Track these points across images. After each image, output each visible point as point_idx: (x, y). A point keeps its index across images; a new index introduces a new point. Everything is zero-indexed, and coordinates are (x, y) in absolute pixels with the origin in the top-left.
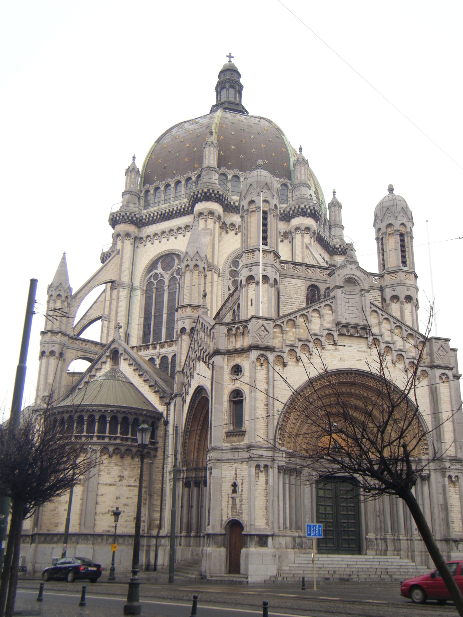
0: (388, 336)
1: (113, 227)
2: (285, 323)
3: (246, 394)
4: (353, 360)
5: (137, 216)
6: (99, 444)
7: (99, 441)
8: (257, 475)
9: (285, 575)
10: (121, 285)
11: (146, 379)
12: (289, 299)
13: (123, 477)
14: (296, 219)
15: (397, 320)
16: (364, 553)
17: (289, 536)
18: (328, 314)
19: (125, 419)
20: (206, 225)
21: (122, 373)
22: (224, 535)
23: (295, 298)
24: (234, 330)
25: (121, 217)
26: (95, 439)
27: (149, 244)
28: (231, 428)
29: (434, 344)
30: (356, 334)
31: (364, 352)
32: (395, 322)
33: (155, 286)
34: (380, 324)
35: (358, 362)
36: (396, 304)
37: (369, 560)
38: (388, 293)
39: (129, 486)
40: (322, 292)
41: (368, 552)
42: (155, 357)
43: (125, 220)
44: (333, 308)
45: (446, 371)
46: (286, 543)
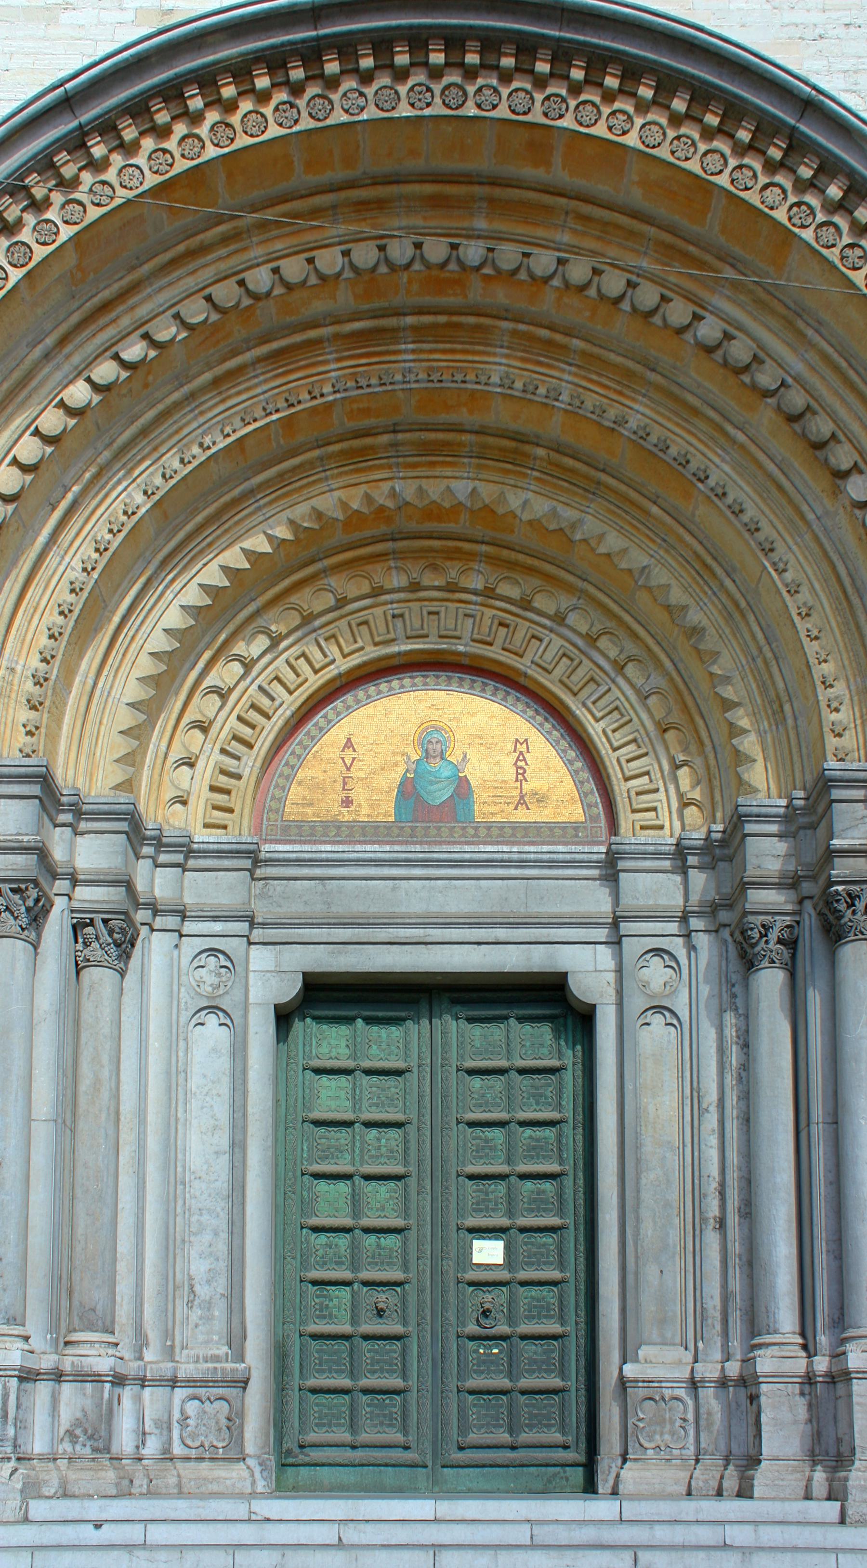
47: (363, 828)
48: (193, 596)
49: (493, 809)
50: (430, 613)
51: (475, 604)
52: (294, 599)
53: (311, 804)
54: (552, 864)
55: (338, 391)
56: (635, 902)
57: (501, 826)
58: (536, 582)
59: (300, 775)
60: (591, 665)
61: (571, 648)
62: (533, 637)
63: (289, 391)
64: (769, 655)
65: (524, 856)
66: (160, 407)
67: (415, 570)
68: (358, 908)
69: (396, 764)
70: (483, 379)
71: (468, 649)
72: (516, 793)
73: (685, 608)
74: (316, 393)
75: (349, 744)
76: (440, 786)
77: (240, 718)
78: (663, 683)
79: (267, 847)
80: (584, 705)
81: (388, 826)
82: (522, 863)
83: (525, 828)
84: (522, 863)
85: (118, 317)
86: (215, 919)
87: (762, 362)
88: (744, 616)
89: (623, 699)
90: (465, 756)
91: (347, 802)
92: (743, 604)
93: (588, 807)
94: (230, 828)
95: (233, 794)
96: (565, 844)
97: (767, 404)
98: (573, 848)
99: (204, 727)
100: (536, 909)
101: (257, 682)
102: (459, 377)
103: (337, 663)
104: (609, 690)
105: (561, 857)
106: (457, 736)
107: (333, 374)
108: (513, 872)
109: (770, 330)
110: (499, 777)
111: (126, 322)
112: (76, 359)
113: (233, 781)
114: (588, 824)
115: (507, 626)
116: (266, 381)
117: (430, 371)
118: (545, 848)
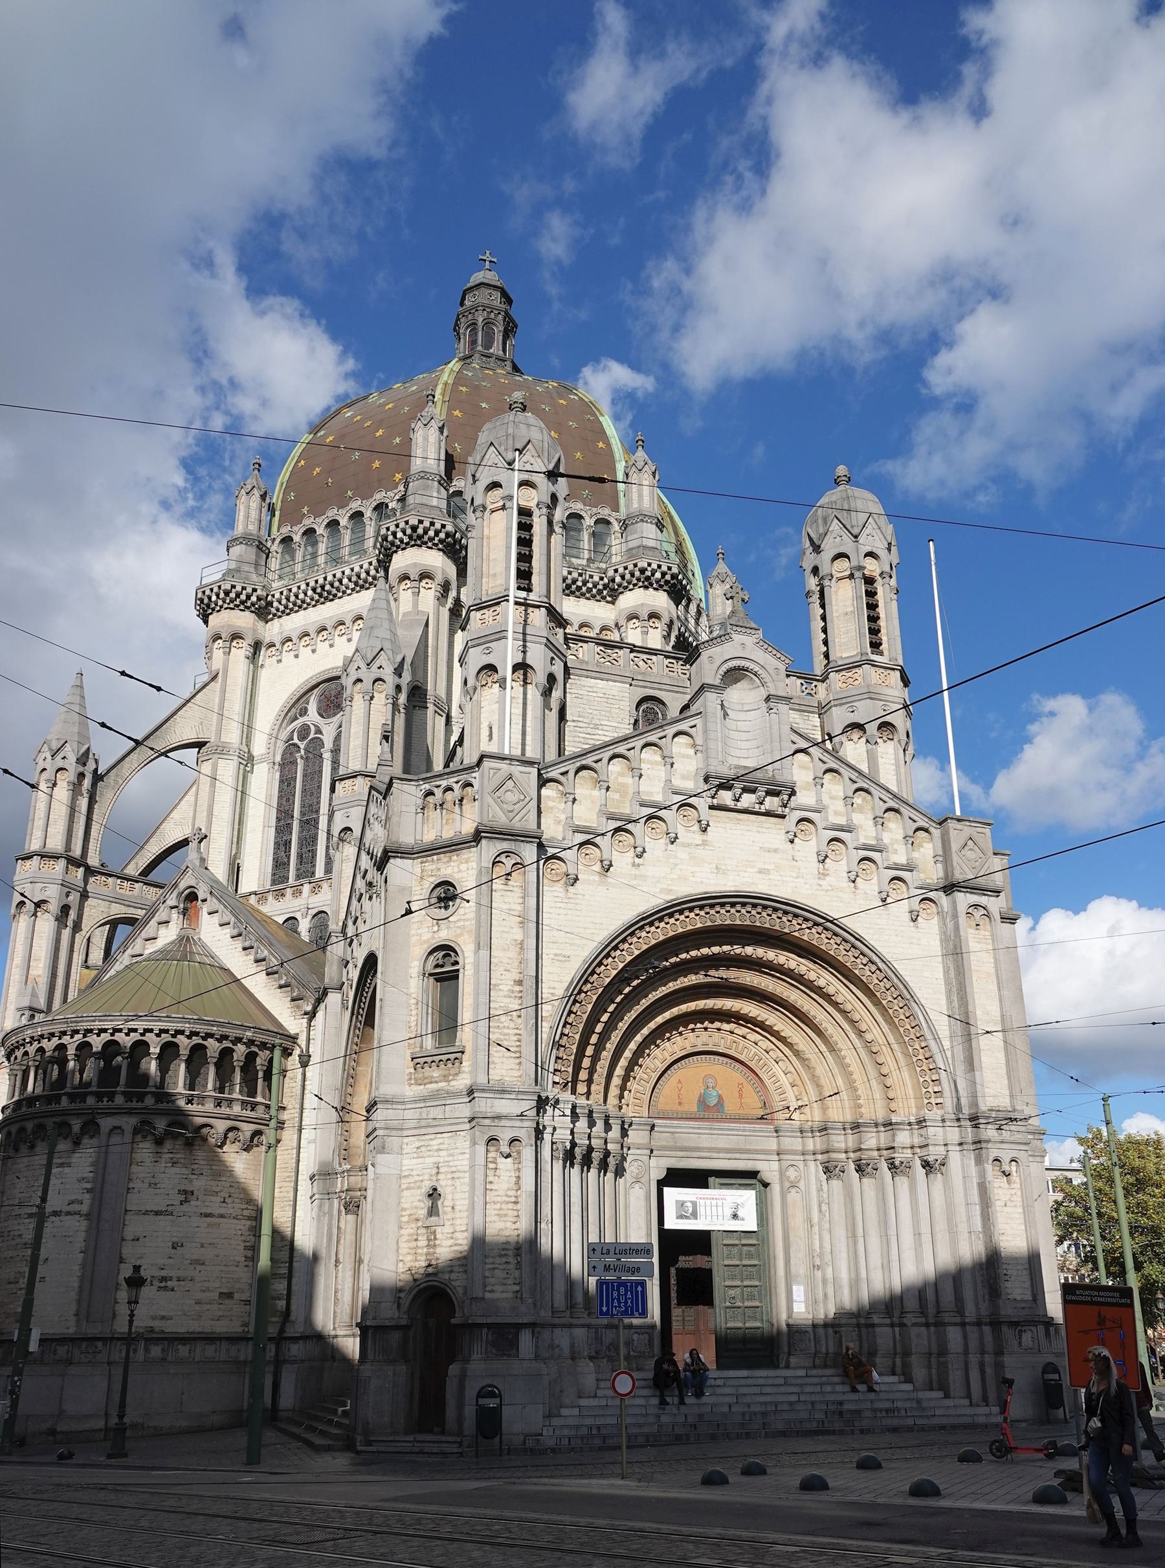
0: (836, 813)
1: (206, 622)
2: (571, 774)
3: (466, 955)
4: (749, 870)
5: (259, 592)
6: (130, 1112)
7: (129, 1105)
8: (491, 1166)
9: (566, 1432)
10: (222, 751)
11: (260, 956)
12: (589, 730)
13: (192, 1192)
14: (628, 594)
15: (860, 773)
16: (783, 1364)
17: (583, 1326)
18: (684, 756)
19: (198, 1052)
20: (416, 604)
21: (204, 946)
22: (406, 1328)
23: (605, 728)
24: (438, 792)
25: (222, 595)
26: (119, 1100)
27: (287, 657)
28: (429, 1043)
29: (953, 833)
30: (757, 806)
31: (776, 851)
32: (854, 778)
33: (302, 752)
34: (818, 782)
35: (762, 876)
36: (858, 746)
37: (793, 1381)
38: (839, 718)
39: (207, 1215)
40: (673, 711)
41: (793, 1360)
42: (298, 916)
43: (232, 601)
44: (699, 741)
45: (983, 900)
46: (572, 1346)
82: (744, 1131)
91: (680, 1104)
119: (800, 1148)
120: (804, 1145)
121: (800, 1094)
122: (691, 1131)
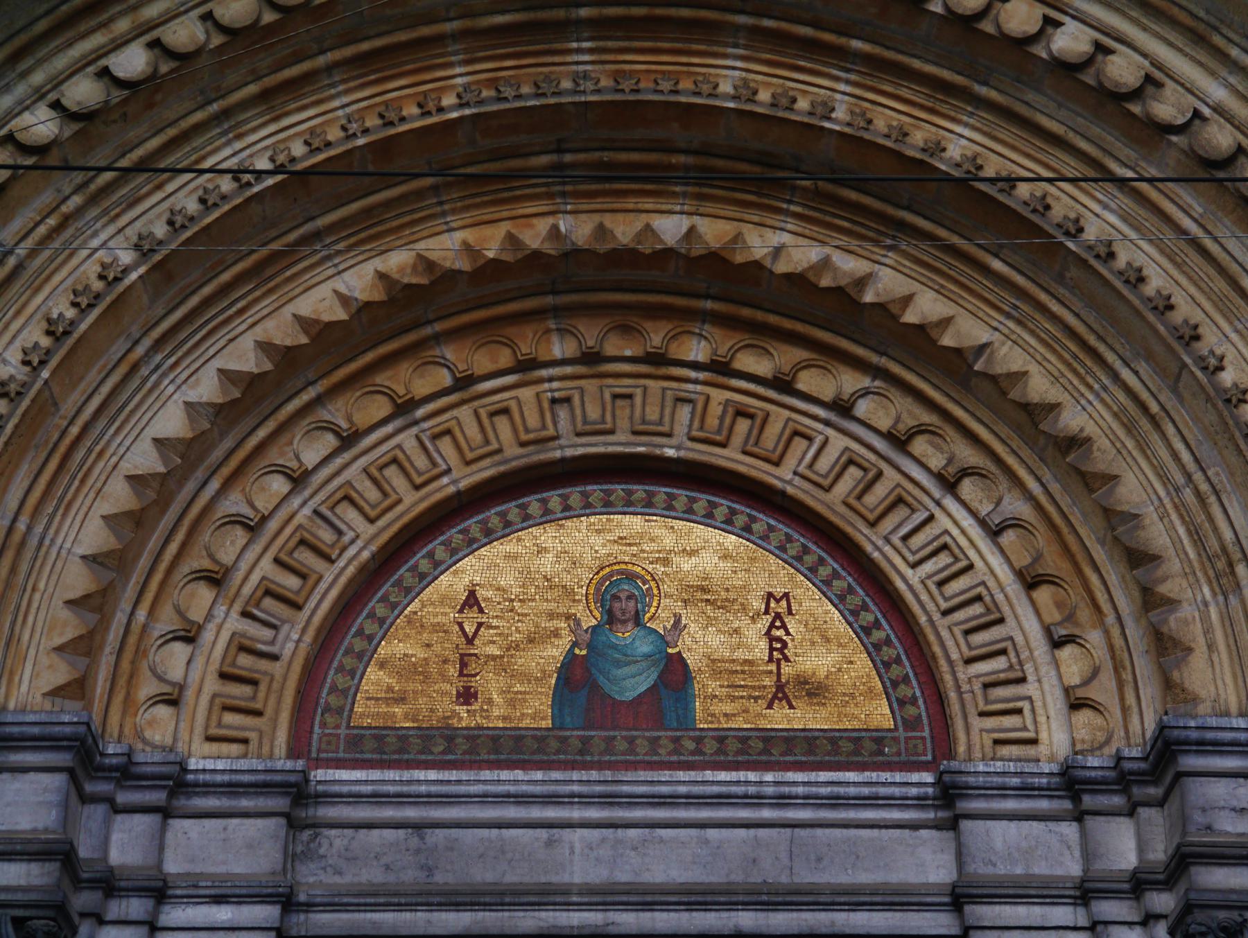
47: (495, 739)
48: (206, 388)
49: (728, 708)
50: (616, 397)
51: (696, 382)
52: (381, 379)
53: (401, 700)
54: (836, 802)
55: (467, 105)
56: (989, 870)
57: (744, 738)
58: (800, 354)
59: (383, 651)
60: (898, 477)
61: (863, 451)
62: (796, 433)
63: (386, 103)
64: (1204, 487)
65: (786, 790)
66: (172, 132)
67: (591, 333)
68: (484, 875)
69: (556, 634)
70: (706, 88)
71: (682, 454)
72: (767, 681)
73: (1054, 407)
74: (431, 106)
75: (472, 601)
76: (632, 669)
77: (277, 561)
78: (1023, 510)
79: (320, 774)
80: (887, 540)
81: (540, 737)
82: (783, 800)
83: (786, 739)
84: (783, 800)
85: (111, 20)
86: (219, 900)
87: (1159, 85)
88: (1157, 425)
89: (955, 532)
90: (678, 619)
92: (1154, 408)
93: (899, 704)
94: (253, 746)
95: (263, 687)
96: (861, 767)
97: (1170, 143)
98: (873, 776)
99: (216, 579)
100: (806, 876)
101: (312, 504)
102: (666, 85)
103: (455, 474)
104: (931, 518)
105: (852, 791)
106: (665, 588)
107: (459, 80)
108: (767, 814)
109: (1171, 44)
110: (740, 654)
111: (123, 25)
112: (38, 78)
113: (264, 664)
114: (901, 733)
115: (751, 416)
116: (347, 92)
117: (617, 76)
118: (824, 776)
119: (1073, 868)
120: (1088, 854)
121: (1070, 618)
122: (512, 812)
